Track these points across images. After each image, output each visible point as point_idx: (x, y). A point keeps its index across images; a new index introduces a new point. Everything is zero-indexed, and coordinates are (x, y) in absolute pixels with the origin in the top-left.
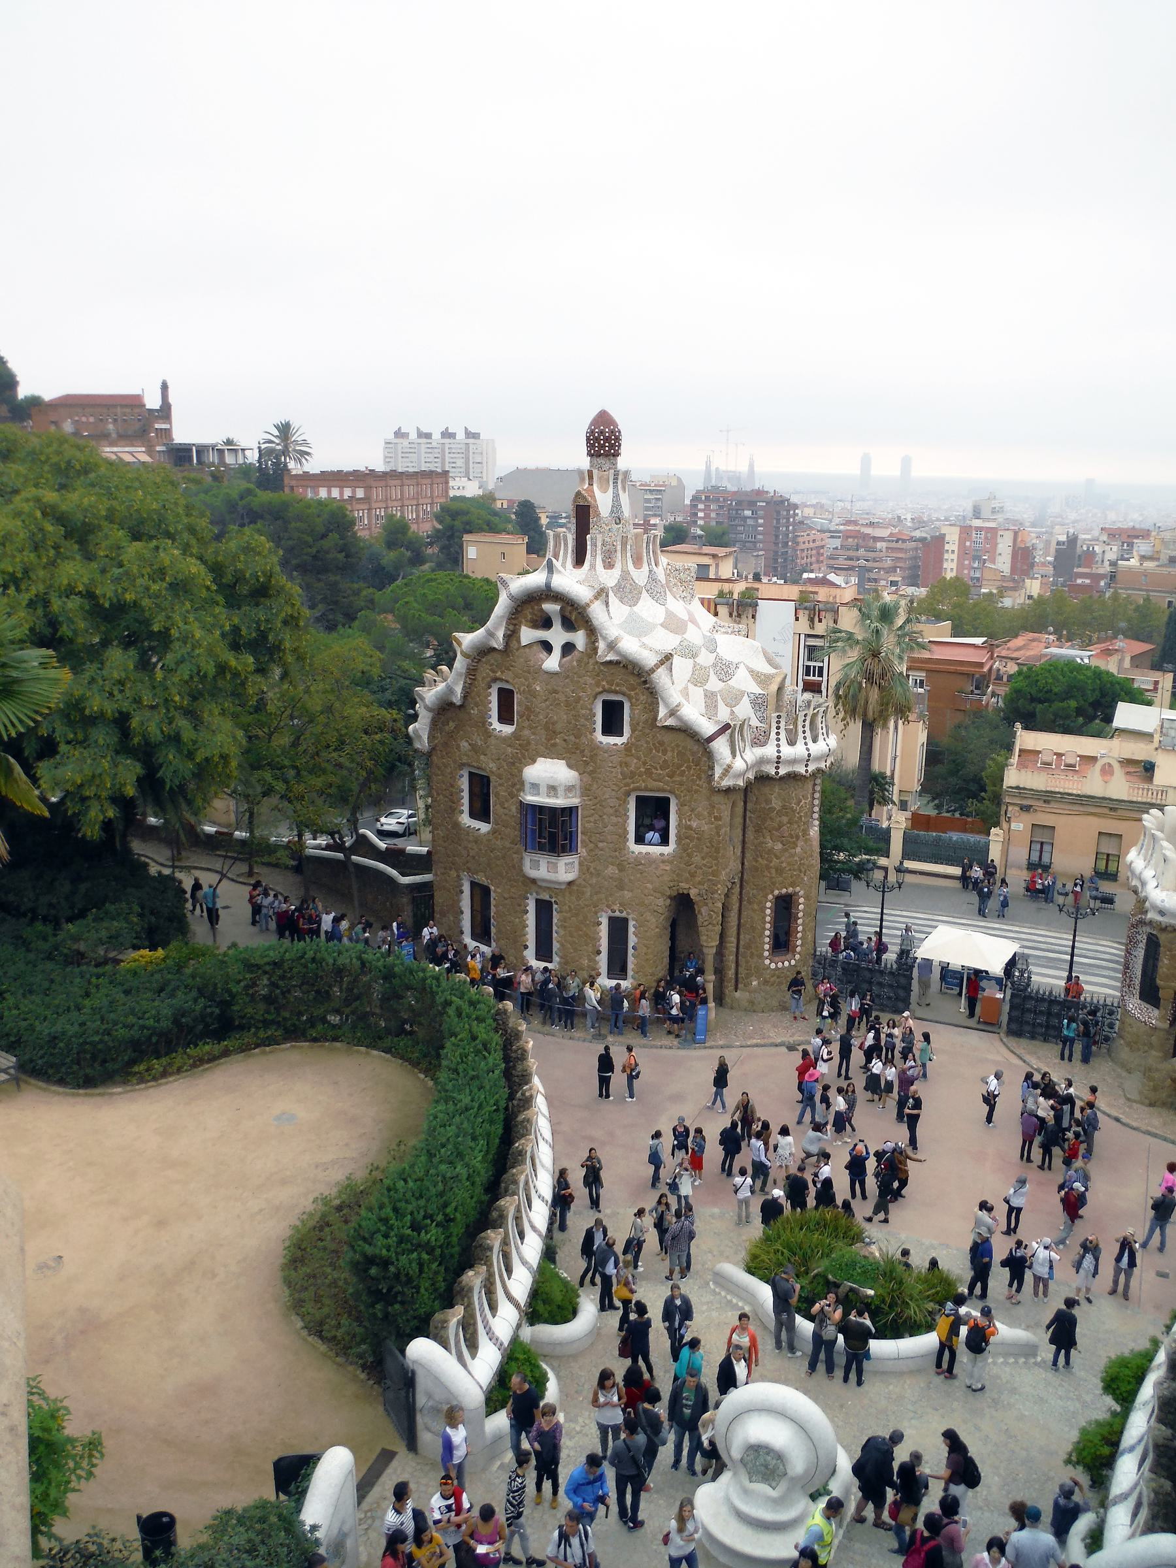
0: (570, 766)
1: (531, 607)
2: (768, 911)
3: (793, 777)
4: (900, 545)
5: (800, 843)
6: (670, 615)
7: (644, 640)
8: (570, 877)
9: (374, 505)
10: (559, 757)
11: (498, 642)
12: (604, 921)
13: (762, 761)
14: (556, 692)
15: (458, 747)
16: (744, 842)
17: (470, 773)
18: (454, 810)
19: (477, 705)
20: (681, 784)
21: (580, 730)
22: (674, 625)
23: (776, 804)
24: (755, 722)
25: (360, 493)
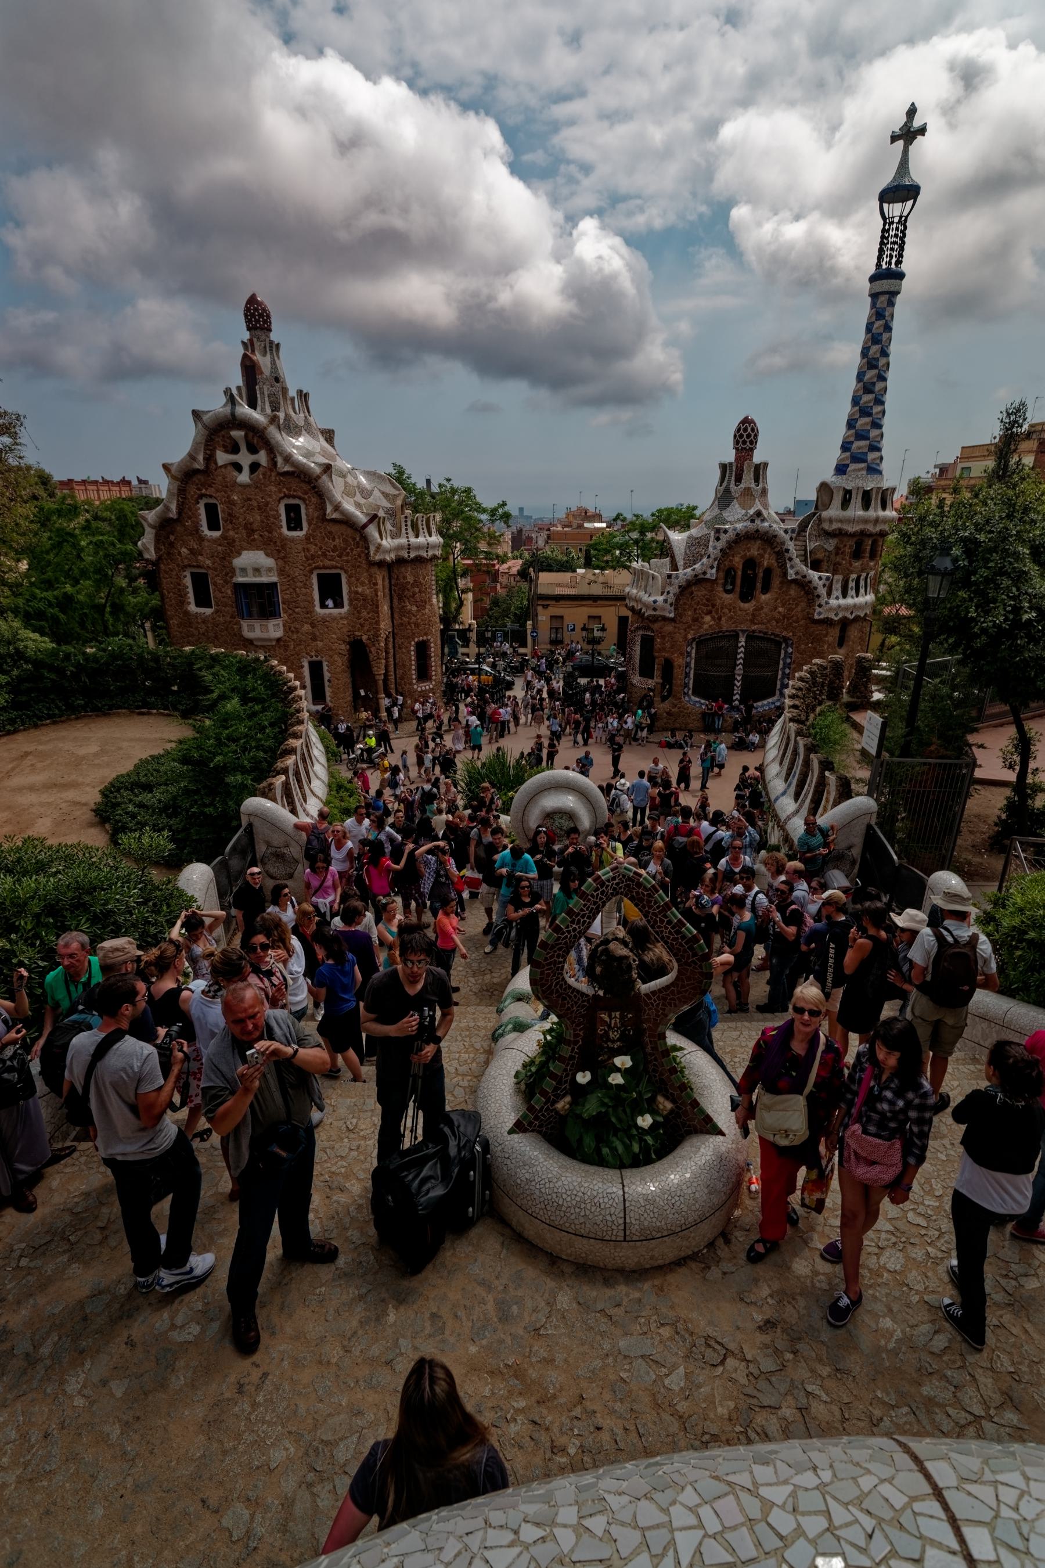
0: (267, 555)
3: (419, 560)
8: (279, 633)
10: (258, 548)
11: (200, 464)
12: (306, 664)
13: (399, 548)
14: (249, 499)
15: (179, 553)
16: (392, 608)
17: (192, 574)
18: (182, 602)
19: (190, 518)
20: (347, 561)
21: (270, 527)
23: (410, 579)
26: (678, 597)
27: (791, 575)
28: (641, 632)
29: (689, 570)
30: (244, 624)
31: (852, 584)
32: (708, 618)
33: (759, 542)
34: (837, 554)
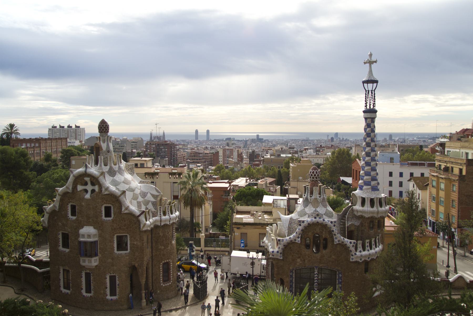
0: (95, 228)
1: (80, 179)
2: (161, 268)
3: (165, 225)
4: (206, 155)
5: (169, 246)
6: (125, 179)
7: (117, 187)
8: (96, 264)
9: (42, 149)
11: (70, 190)
12: (108, 277)
15: (58, 225)
17: (63, 234)
18: (57, 245)
22: (126, 182)
24: (153, 210)
25: (37, 145)
26: (284, 250)
27: (336, 241)
28: (271, 260)
29: (288, 238)
30: (81, 259)
31: (367, 244)
32: (299, 260)
33: (319, 226)
34: (362, 226)
